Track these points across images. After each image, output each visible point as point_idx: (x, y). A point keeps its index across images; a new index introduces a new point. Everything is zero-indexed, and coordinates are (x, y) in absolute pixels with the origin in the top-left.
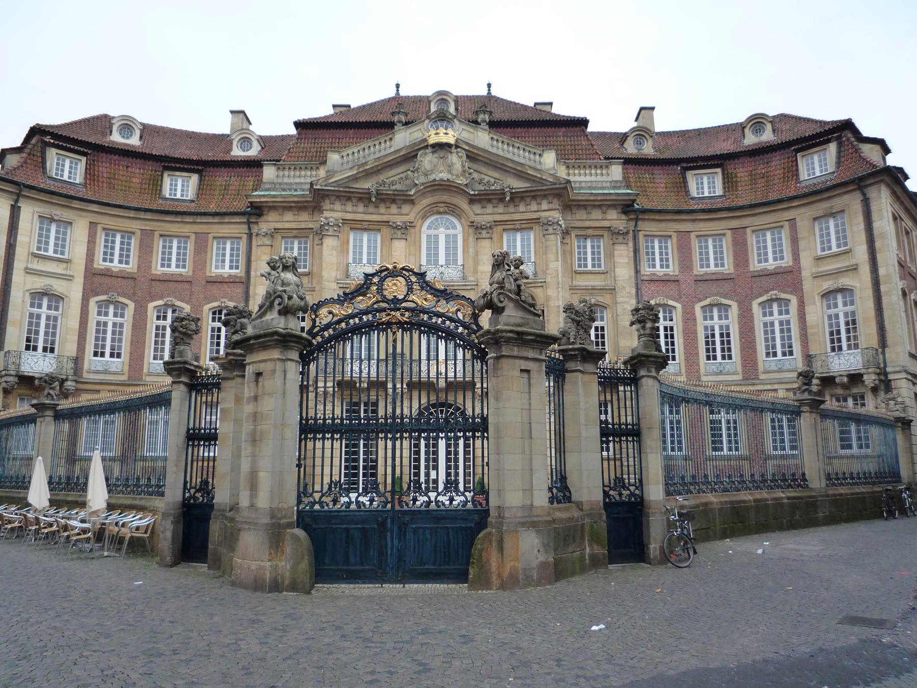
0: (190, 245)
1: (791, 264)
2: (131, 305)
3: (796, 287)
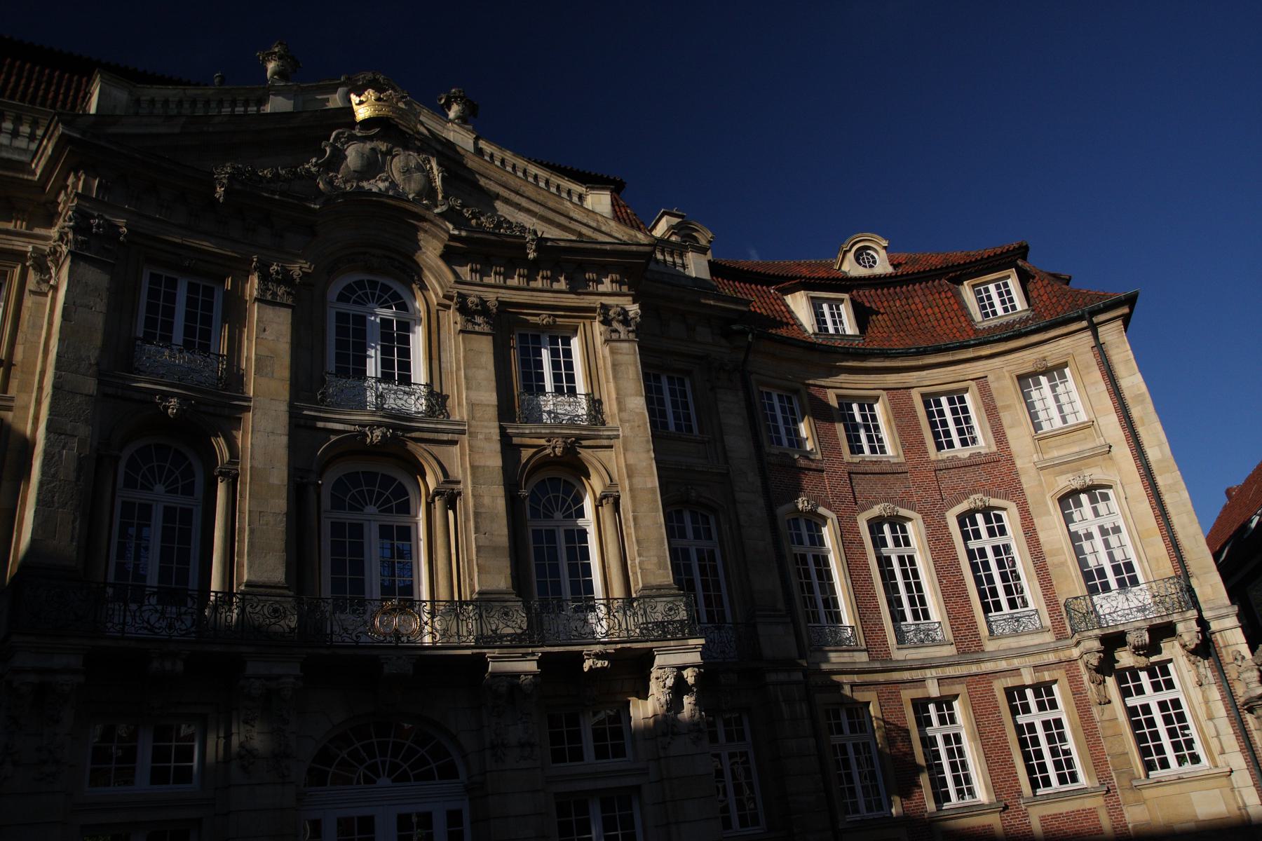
3: (1014, 490)
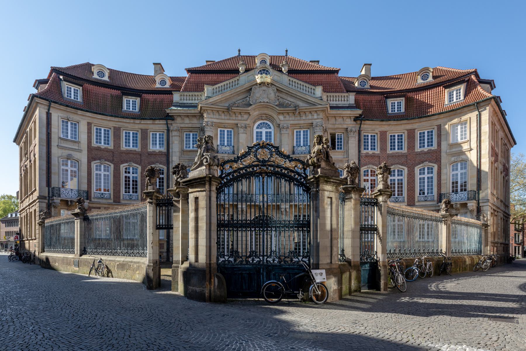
1: (436, 148)
2: (112, 166)
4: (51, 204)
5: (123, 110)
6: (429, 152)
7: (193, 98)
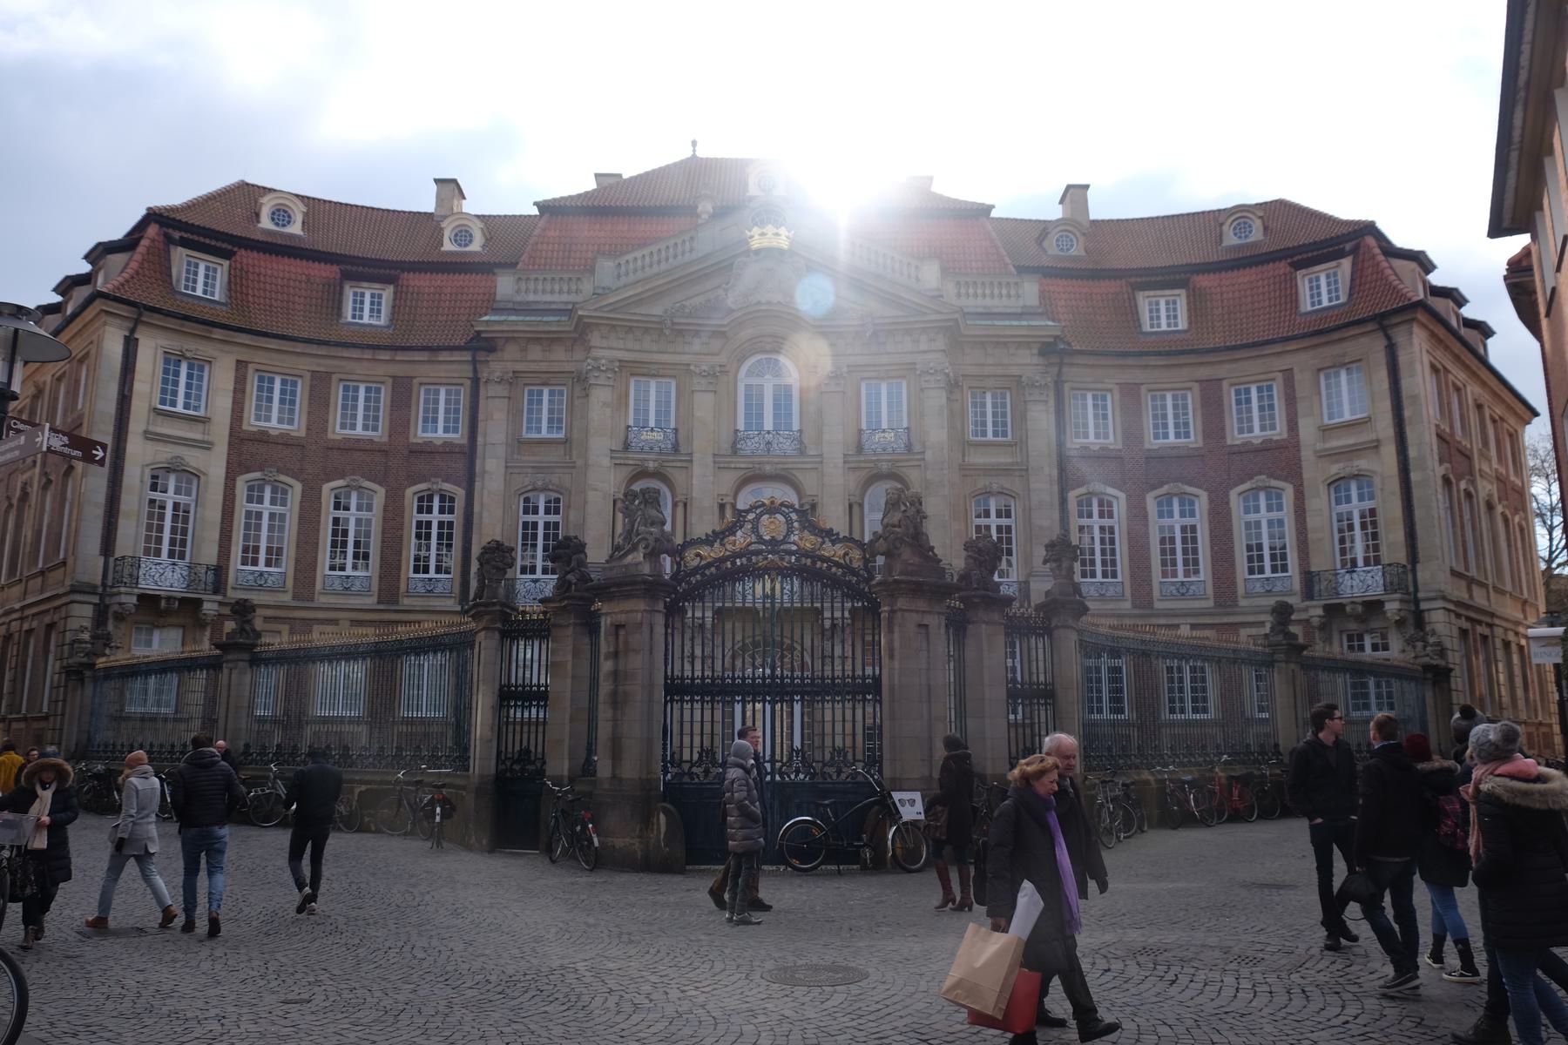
0: (385, 396)
1: (1285, 436)
2: (298, 487)
3: (1293, 472)
4: (107, 607)
5: (343, 321)
6: (1267, 447)
7: (557, 287)
